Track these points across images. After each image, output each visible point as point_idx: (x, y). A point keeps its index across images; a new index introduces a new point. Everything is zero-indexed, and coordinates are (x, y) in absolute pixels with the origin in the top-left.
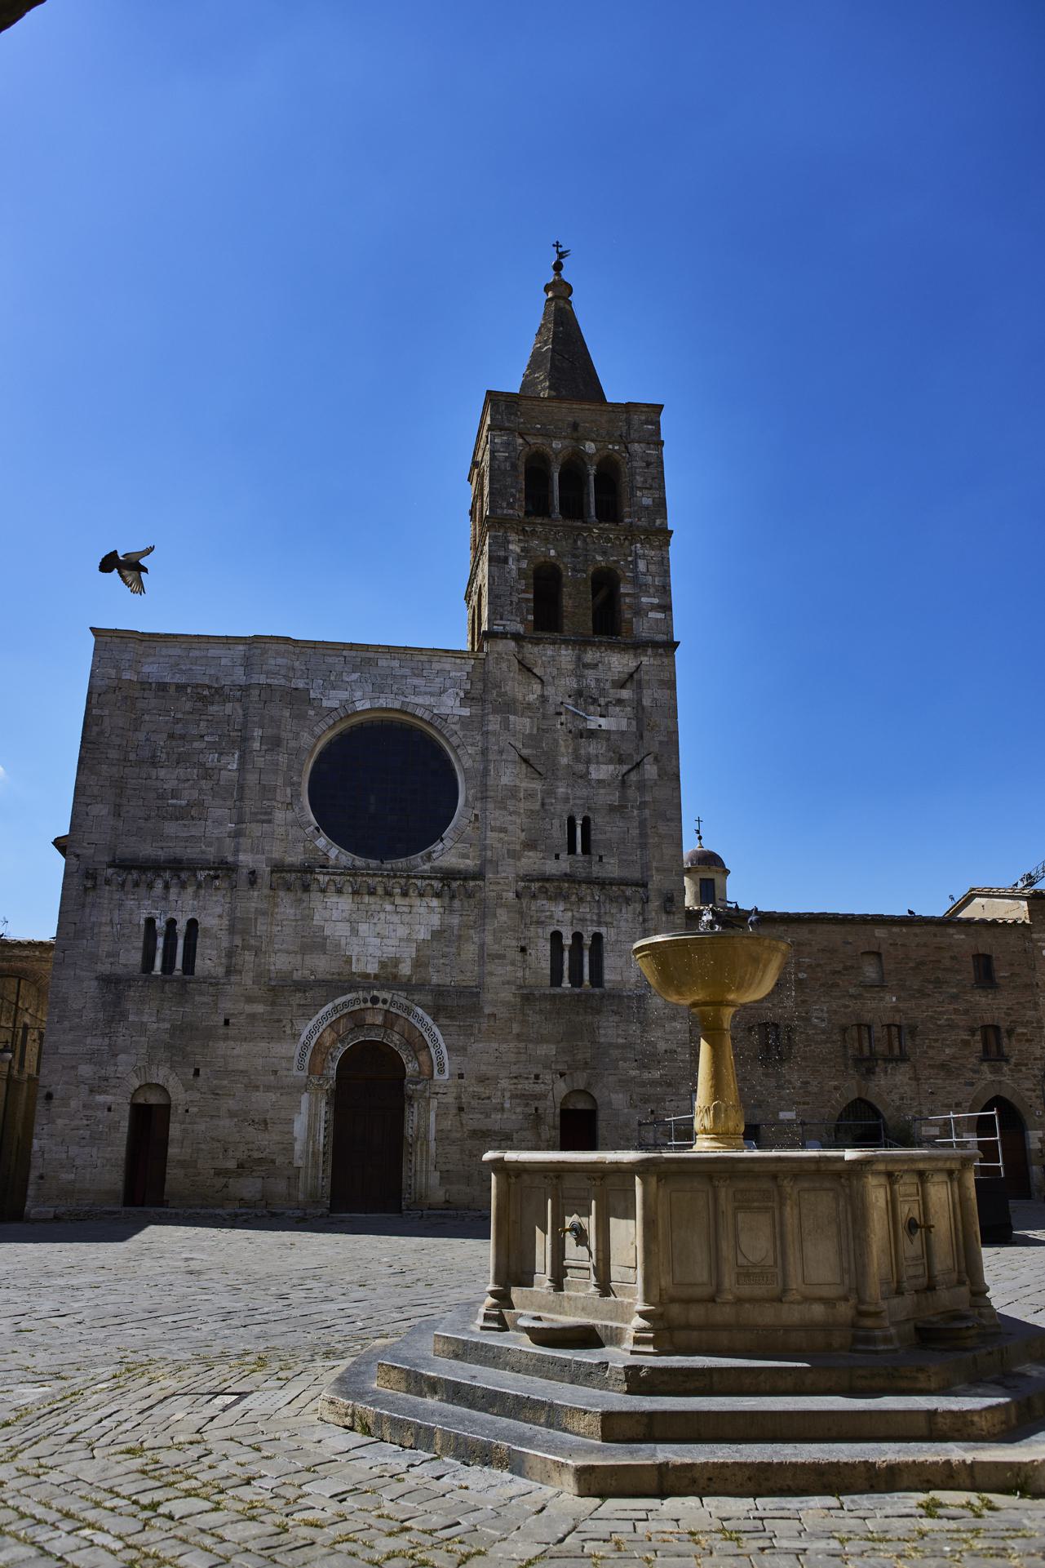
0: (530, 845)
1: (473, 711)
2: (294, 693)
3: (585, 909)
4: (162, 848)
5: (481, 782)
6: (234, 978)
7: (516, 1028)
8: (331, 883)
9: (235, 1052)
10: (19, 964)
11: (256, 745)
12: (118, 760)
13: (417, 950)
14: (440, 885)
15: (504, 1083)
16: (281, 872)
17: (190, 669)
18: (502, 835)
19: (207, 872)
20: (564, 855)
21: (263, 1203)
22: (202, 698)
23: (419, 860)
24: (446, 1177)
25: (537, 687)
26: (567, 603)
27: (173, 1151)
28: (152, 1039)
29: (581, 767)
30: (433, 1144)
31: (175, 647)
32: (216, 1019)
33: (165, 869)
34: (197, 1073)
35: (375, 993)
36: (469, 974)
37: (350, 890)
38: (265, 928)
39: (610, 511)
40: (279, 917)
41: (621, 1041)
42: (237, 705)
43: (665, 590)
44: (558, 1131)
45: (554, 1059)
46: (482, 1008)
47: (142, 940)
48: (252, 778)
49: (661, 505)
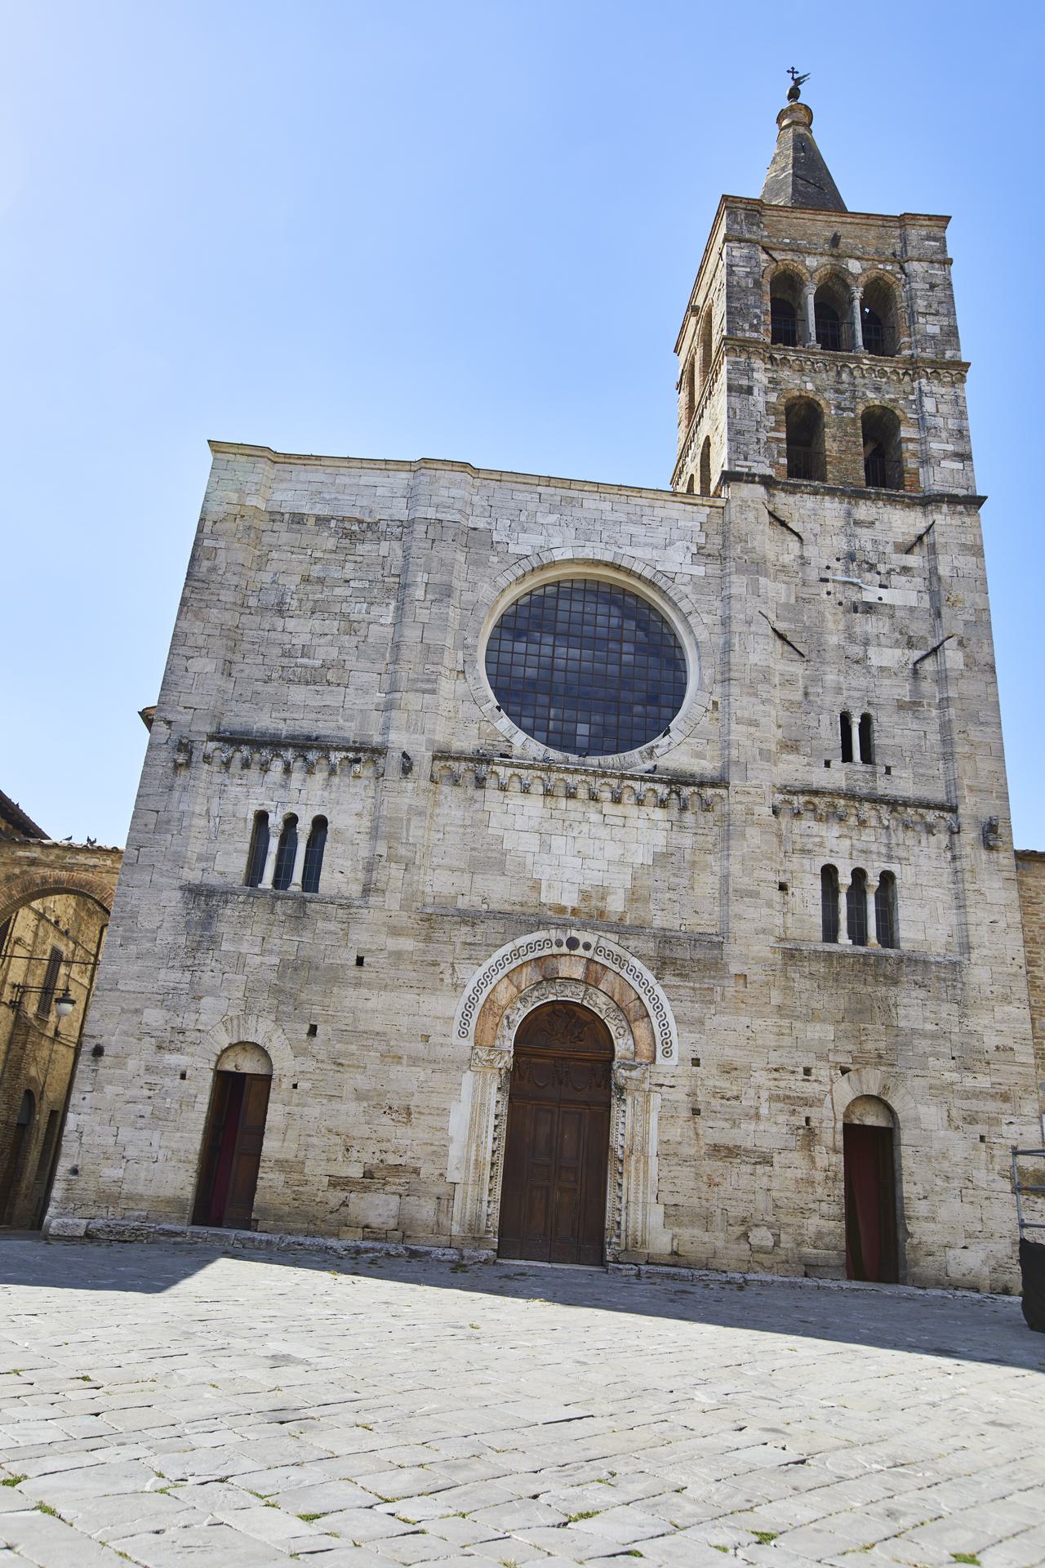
0: (791, 746)
1: (710, 571)
2: (471, 533)
3: (868, 836)
4: (285, 720)
5: (721, 660)
6: (373, 900)
7: (776, 997)
8: (515, 779)
9: (370, 1005)
10: (84, 876)
11: (419, 593)
12: (235, 603)
14: (667, 791)
15: (760, 1078)
16: (447, 759)
18: (752, 729)
20: (837, 763)
21: (398, 1234)
22: (349, 535)
23: (637, 756)
24: (673, 1215)
25: (793, 544)
26: (831, 446)
27: (271, 1146)
28: (251, 978)
29: (856, 650)
30: (654, 1162)
33: (286, 746)
34: (313, 1031)
35: (574, 933)
36: (706, 916)
37: (541, 790)
38: (420, 832)
39: (880, 338)
40: (441, 820)
41: (930, 1027)
42: (396, 545)
43: (961, 434)
44: (841, 1157)
45: (831, 1046)
46: (726, 964)
48: (411, 634)
49: (951, 334)
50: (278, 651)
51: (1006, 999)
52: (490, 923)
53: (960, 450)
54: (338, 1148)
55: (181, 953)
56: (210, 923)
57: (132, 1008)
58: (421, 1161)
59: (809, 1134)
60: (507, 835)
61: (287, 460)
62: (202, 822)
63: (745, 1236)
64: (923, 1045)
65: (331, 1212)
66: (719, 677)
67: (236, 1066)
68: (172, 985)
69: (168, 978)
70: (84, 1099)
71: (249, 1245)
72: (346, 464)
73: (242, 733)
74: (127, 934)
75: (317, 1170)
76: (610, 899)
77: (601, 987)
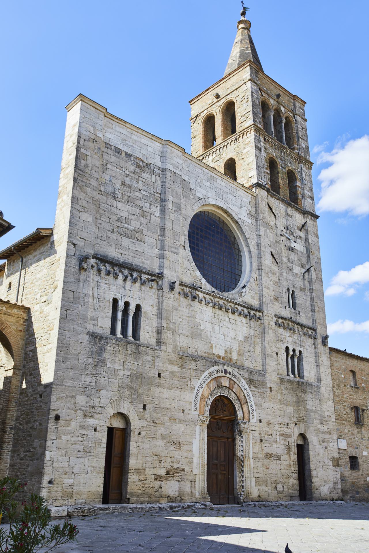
6: (163, 347)
11: (170, 206)
12: (97, 188)
13: (239, 346)
15: (277, 427)
17: (132, 146)
19: (147, 276)
20: (287, 307)
22: (139, 167)
27: (133, 463)
28: (120, 382)
29: (290, 265)
30: (252, 460)
31: (123, 128)
32: (154, 372)
33: (125, 268)
34: (144, 407)
35: (226, 368)
36: (259, 364)
42: (158, 178)
47: (111, 312)
48: (168, 225)
50: (114, 218)
51: (329, 399)
52: (201, 361)
53: (311, 196)
54: (157, 462)
55: (90, 367)
56: (102, 353)
57: (71, 395)
58: (185, 466)
59: (288, 447)
60: (202, 322)
61: (111, 117)
62: (91, 300)
63: (276, 487)
64: (312, 414)
65: (156, 491)
66: (257, 267)
67: (111, 424)
68: (87, 383)
69: (86, 380)
70: (53, 443)
71: (135, 511)
72: (136, 130)
73: (104, 256)
74: (66, 356)
75: (150, 473)
76: (233, 353)
77: (234, 390)
